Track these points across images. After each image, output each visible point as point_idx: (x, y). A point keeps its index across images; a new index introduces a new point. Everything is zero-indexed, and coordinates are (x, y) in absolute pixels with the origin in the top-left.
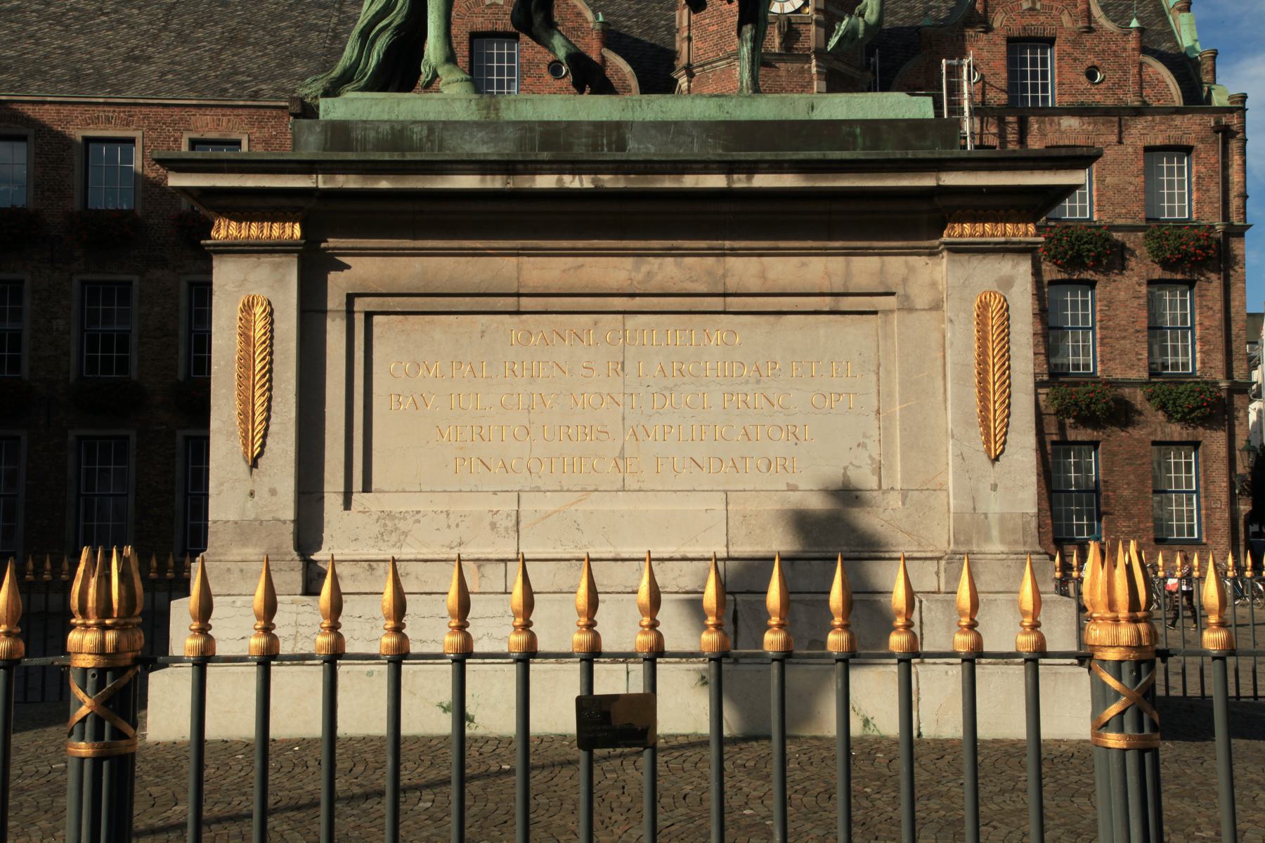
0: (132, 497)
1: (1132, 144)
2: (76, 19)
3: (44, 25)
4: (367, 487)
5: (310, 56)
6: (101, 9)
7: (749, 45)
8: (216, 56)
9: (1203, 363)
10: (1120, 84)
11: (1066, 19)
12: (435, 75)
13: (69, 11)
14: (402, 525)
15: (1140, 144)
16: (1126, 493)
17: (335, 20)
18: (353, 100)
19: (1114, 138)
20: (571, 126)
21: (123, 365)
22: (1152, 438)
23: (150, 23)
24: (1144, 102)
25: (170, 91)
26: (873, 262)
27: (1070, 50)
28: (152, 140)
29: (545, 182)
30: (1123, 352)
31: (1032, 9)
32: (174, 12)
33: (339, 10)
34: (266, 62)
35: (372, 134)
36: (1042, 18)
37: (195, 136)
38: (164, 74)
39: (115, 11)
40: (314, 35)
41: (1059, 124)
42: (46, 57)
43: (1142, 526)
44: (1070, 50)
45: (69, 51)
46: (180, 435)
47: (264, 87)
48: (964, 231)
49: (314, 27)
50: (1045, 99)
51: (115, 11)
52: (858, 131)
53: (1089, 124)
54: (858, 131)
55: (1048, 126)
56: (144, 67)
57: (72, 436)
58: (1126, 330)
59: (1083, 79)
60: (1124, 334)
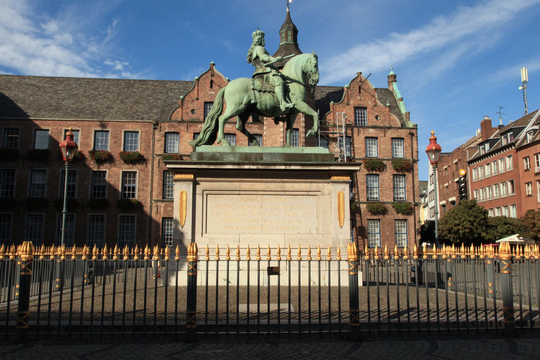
0: (105, 233)
1: (388, 137)
2: (93, 97)
3: (84, 98)
4: (206, 233)
5: (158, 107)
6: (99, 94)
7: (289, 134)
8: (132, 107)
9: (408, 197)
10: (384, 121)
11: (370, 103)
12: (220, 141)
13: (91, 94)
14: (214, 241)
15: (390, 137)
16: (388, 234)
17: (165, 97)
18: (203, 147)
19: (383, 135)
20: (251, 154)
21: (103, 195)
22: (394, 218)
23: (113, 98)
24: (391, 126)
25: (119, 117)
26: (316, 184)
27: (371, 111)
29: (246, 167)
30: (386, 194)
31: (360, 99)
32: (120, 94)
33: (166, 94)
34: (146, 109)
35: (208, 155)
36: (363, 102)
37: (126, 130)
38: (117, 112)
39: (104, 94)
40: (159, 101)
41: (368, 131)
42: (84, 107)
43: (392, 243)
44: (371, 111)
45: (91, 106)
46: (119, 215)
47: (145, 116)
48: (334, 178)
49: (159, 99)
50: (365, 124)
51: (104, 94)
52: (313, 156)
53: (376, 131)
54: (313, 156)
55: (366, 131)
56: (111, 110)
57: (88, 215)
58: (387, 188)
59: (375, 119)
60: (387, 189)
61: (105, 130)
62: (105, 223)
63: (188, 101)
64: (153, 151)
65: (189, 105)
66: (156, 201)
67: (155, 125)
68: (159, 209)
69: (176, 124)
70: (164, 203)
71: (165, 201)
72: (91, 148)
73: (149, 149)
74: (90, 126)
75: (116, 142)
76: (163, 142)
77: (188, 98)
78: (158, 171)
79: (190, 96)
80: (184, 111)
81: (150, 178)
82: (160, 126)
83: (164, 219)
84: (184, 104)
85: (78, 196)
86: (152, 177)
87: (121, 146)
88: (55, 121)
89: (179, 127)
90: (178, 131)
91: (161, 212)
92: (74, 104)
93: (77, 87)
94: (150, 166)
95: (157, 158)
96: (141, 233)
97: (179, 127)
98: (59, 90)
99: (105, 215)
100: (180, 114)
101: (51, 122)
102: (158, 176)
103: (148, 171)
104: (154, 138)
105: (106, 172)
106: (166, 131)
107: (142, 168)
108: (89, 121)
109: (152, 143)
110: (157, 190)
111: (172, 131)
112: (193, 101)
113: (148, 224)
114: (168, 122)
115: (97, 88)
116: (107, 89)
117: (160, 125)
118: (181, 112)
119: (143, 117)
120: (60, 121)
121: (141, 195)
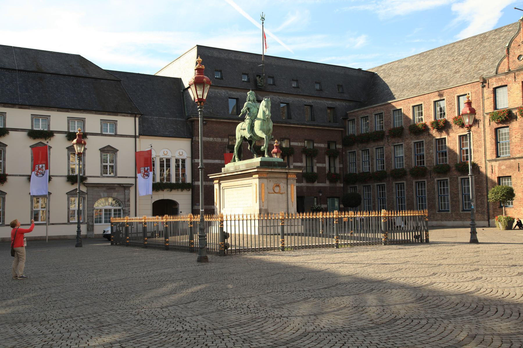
0: (449, 196)
6: (453, 59)
21: (446, 161)
28: (448, 98)
37: (458, 95)
38: (461, 75)
42: (436, 78)
45: (441, 75)
46: (459, 178)
57: (436, 179)
61: (442, 98)
62: (449, 186)
63: (514, 47)
64: (483, 111)
65: (516, 51)
66: (490, 161)
67: (483, 83)
68: (493, 169)
69: (503, 77)
70: (498, 162)
71: (499, 160)
72: (433, 120)
73: (480, 109)
74: (429, 98)
75: (451, 109)
76: (492, 99)
77: (514, 44)
78: (489, 130)
79: (516, 41)
80: (511, 60)
81: (483, 138)
82: (487, 83)
83: (499, 178)
84: (510, 53)
85: (426, 164)
86: (485, 136)
87: (455, 111)
88: (404, 100)
89: (507, 79)
90: (506, 84)
91: (496, 172)
92: (429, 77)
93: (437, 57)
94: (481, 126)
95: (488, 117)
96: (479, 194)
97: (507, 79)
98: (423, 66)
99: (448, 178)
100: (507, 64)
101: (402, 101)
102: (490, 135)
103: (480, 132)
104: (483, 97)
105: (445, 138)
106: (494, 86)
107: (475, 130)
108: (428, 93)
109: (482, 102)
110: (490, 149)
111: (500, 85)
112: (519, 45)
113: (485, 185)
114: (495, 76)
115: (453, 53)
116: (461, 51)
117: (487, 81)
118: (508, 61)
119: (482, 75)
120: (408, 99)
121: (476, 156)
